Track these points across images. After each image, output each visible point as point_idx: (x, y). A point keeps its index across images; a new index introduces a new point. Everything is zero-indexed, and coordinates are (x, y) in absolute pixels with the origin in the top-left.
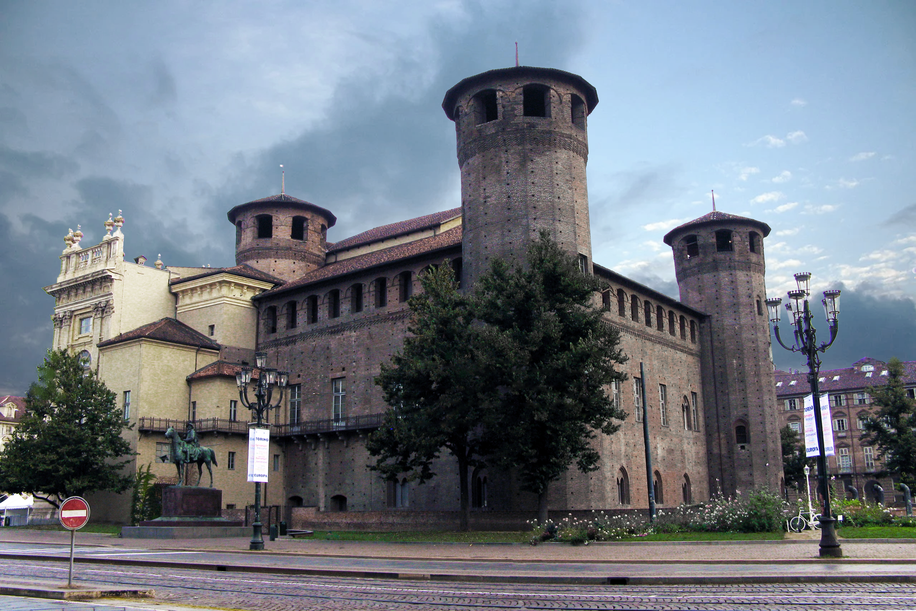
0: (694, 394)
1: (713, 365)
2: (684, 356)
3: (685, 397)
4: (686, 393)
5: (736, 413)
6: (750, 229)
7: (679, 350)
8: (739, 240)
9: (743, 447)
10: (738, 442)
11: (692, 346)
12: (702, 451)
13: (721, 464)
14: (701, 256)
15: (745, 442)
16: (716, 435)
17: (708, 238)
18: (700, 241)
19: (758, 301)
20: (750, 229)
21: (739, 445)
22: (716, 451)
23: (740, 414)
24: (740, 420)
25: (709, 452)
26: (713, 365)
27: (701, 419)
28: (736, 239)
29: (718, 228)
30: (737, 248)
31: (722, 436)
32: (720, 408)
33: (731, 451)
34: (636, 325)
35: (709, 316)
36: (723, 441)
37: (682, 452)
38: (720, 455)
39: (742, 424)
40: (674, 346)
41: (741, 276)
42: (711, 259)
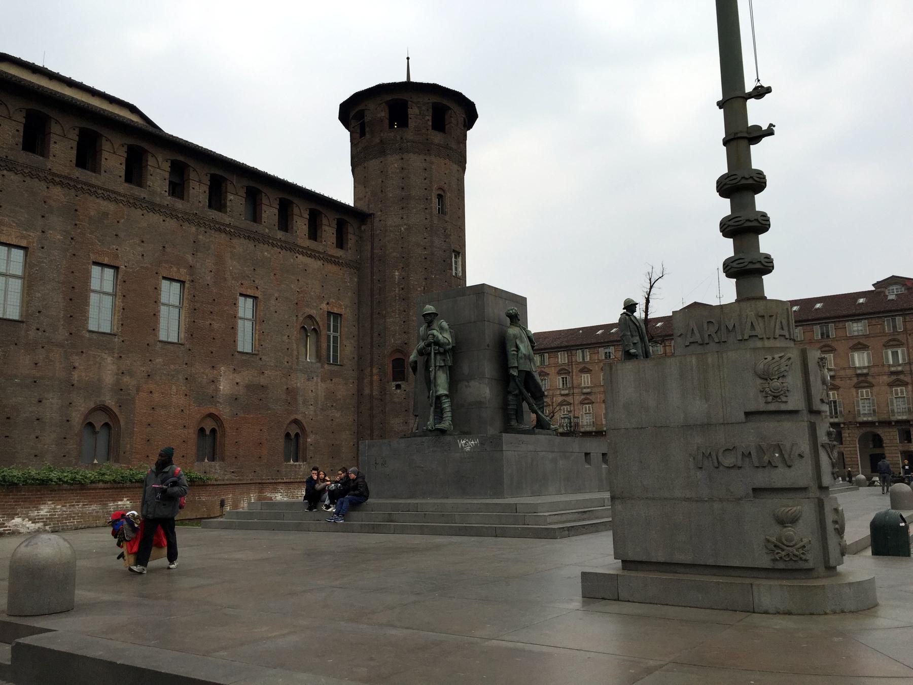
0: (337, 316)
1: (372, 280)
2: (314, 264)
3: (310, 317)
4: (313, 312)
5: (394, 341)
6: (437, 99)
7: (303, 254)
8: (419, 113)
9: (398, 387)
10: (394, 380)
11: (339, 253)
12: (344, 389)
13: (371, 409)
14: (368, 136)
15: (403, 379)
16: (369, 369)
17: (378, 111)
18: (368, 118)
19: (440, 197)
20: (437, 99)
21: (394, 383)
22: (367, 391)
23: (398, 342)
24: (398, 351)
25: (360, 392)
26: (372, 280)
27: (347, 349)
28: (413, 111)
29: (389, 98)
30: (412, 123)
31: (375, 371)
32: (376, 334)
33: (383, 391)
34: (179, 204)
35: (371, 215)
36: (375, 378)
37: (291, 393)
38: (371, 396)
39: (401, 356)
40: (292, 248)
41: (416, 161)
42: (378, 140)
